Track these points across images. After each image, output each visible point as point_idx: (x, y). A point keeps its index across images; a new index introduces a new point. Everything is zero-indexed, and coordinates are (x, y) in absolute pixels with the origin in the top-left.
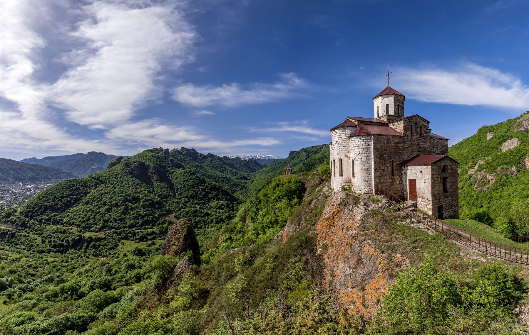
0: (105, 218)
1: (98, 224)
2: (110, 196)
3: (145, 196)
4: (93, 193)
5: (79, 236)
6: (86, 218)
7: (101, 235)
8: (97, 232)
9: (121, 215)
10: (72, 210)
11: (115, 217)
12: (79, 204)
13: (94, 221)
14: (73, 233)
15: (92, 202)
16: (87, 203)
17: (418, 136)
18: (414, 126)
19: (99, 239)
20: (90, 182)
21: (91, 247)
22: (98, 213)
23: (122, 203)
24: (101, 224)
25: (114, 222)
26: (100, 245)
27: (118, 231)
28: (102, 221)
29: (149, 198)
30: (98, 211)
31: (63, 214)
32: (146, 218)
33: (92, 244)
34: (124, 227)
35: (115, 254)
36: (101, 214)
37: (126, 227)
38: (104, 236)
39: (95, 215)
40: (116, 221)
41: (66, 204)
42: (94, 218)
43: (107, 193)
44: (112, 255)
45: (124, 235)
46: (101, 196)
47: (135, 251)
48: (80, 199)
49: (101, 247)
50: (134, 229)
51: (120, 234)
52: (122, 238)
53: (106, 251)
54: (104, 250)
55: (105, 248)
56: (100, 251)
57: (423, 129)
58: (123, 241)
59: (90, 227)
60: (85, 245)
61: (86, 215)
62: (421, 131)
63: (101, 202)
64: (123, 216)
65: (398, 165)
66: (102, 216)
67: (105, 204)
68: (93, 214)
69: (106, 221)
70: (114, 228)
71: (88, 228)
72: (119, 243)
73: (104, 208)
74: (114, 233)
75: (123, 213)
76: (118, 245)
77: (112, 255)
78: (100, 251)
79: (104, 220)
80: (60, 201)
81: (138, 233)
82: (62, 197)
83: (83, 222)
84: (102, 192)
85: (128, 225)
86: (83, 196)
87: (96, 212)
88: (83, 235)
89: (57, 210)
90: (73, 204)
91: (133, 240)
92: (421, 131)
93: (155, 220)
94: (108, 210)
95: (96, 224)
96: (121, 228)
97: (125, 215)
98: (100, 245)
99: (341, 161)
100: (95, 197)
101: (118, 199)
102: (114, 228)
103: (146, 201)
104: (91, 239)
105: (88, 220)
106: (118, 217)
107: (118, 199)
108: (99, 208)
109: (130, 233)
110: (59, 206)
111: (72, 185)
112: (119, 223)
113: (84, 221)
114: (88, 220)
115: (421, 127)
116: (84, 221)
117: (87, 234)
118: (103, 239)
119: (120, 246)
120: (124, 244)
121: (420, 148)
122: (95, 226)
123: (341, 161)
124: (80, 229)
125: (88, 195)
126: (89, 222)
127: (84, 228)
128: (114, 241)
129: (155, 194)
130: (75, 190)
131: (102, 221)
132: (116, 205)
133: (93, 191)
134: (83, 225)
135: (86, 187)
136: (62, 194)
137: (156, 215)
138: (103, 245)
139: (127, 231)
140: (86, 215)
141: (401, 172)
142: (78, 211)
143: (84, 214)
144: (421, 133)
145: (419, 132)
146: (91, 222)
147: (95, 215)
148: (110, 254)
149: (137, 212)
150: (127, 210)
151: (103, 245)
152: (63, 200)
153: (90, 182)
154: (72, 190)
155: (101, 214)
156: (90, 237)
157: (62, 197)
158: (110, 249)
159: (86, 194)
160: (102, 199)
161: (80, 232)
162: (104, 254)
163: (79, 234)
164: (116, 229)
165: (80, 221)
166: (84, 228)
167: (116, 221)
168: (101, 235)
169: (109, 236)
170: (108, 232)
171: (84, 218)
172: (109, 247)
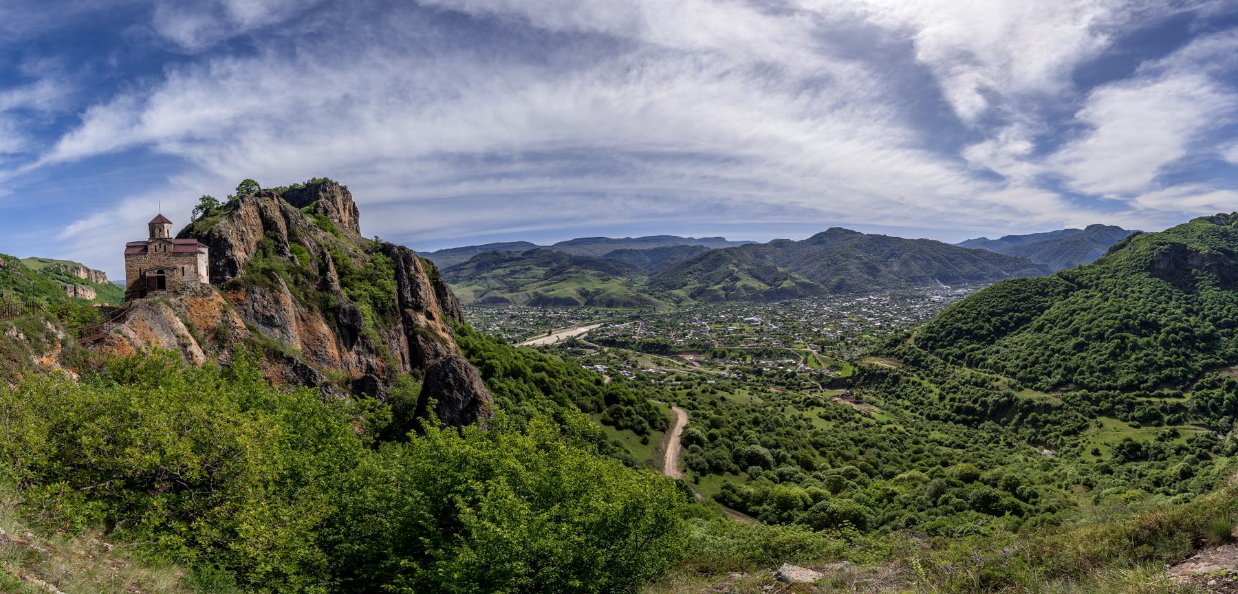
0: (1071, 364)
3: (1175, 319)
4: (1057, 308)
6: (1031, 359)
7: (1054, 399)
8: (1047, 392)
10: (1007, 340)
11: (1093, 364)
16: (1040, 329)
27: (1094, 395)
29: (1185, 325)
30: (1059, 346)
32: (1167, 372)
34: (1109, 388)
38: (1060, 402)
42: (1047, 361)
43: (1085, 310)
45: (1105, 405)
48: (1028, 320)
51: (1096, 402)
52: (1101, 413)
59: (1035, 380)
61: (1031, 354)
63: (1068, 329)
66: (1064, 359)
67: (1075, 332)
68: (1047, 353)
69: (1070, 371)
72: (1092, 423)
73: (1073, 341)
74: (1084, 398)
80: (989, 321)
82: (992, 314)
84: (1075, 306)
87: (1052, 350)
89: (980, 338)
90: (1013, 329)
91: (1125, 420)
93: (1190, 376)
94: (1080, 347)
95: (1049, 374)
96: (1102, 389)
97: (1116, 360)
103: (1175, 331)
105: (1033, 364)
108: (1063, 340)
112: (1098, 377)
113: (1025, 367)
114: (1033, 364)
116: (1025, 367)
120: (1101, 426)
122: (1045, 378)
125: (1046, 312)
128: (1080, 415)
129: (1205, 317)
130: (1019, 301)
131: (1061, 370)
133: (1057, 304)
134: (1021, 374)
135: (1044, 294)
137: (1197, 366)
140: (1031, 354)
142: (1018, 344)
143: (1027, 352)
146: (1038, 368)
149: (1147, 355)
152: (994, 319)
155: (1064, 353)
157: (992, 314)
159: (1042, 310)
160: (1071, 322)
164: (1090, 390)
167: (1092, 373)
168: (1054, 399)
169: (1071, 404)
170: (1072, 394)
171: (1025, 360)
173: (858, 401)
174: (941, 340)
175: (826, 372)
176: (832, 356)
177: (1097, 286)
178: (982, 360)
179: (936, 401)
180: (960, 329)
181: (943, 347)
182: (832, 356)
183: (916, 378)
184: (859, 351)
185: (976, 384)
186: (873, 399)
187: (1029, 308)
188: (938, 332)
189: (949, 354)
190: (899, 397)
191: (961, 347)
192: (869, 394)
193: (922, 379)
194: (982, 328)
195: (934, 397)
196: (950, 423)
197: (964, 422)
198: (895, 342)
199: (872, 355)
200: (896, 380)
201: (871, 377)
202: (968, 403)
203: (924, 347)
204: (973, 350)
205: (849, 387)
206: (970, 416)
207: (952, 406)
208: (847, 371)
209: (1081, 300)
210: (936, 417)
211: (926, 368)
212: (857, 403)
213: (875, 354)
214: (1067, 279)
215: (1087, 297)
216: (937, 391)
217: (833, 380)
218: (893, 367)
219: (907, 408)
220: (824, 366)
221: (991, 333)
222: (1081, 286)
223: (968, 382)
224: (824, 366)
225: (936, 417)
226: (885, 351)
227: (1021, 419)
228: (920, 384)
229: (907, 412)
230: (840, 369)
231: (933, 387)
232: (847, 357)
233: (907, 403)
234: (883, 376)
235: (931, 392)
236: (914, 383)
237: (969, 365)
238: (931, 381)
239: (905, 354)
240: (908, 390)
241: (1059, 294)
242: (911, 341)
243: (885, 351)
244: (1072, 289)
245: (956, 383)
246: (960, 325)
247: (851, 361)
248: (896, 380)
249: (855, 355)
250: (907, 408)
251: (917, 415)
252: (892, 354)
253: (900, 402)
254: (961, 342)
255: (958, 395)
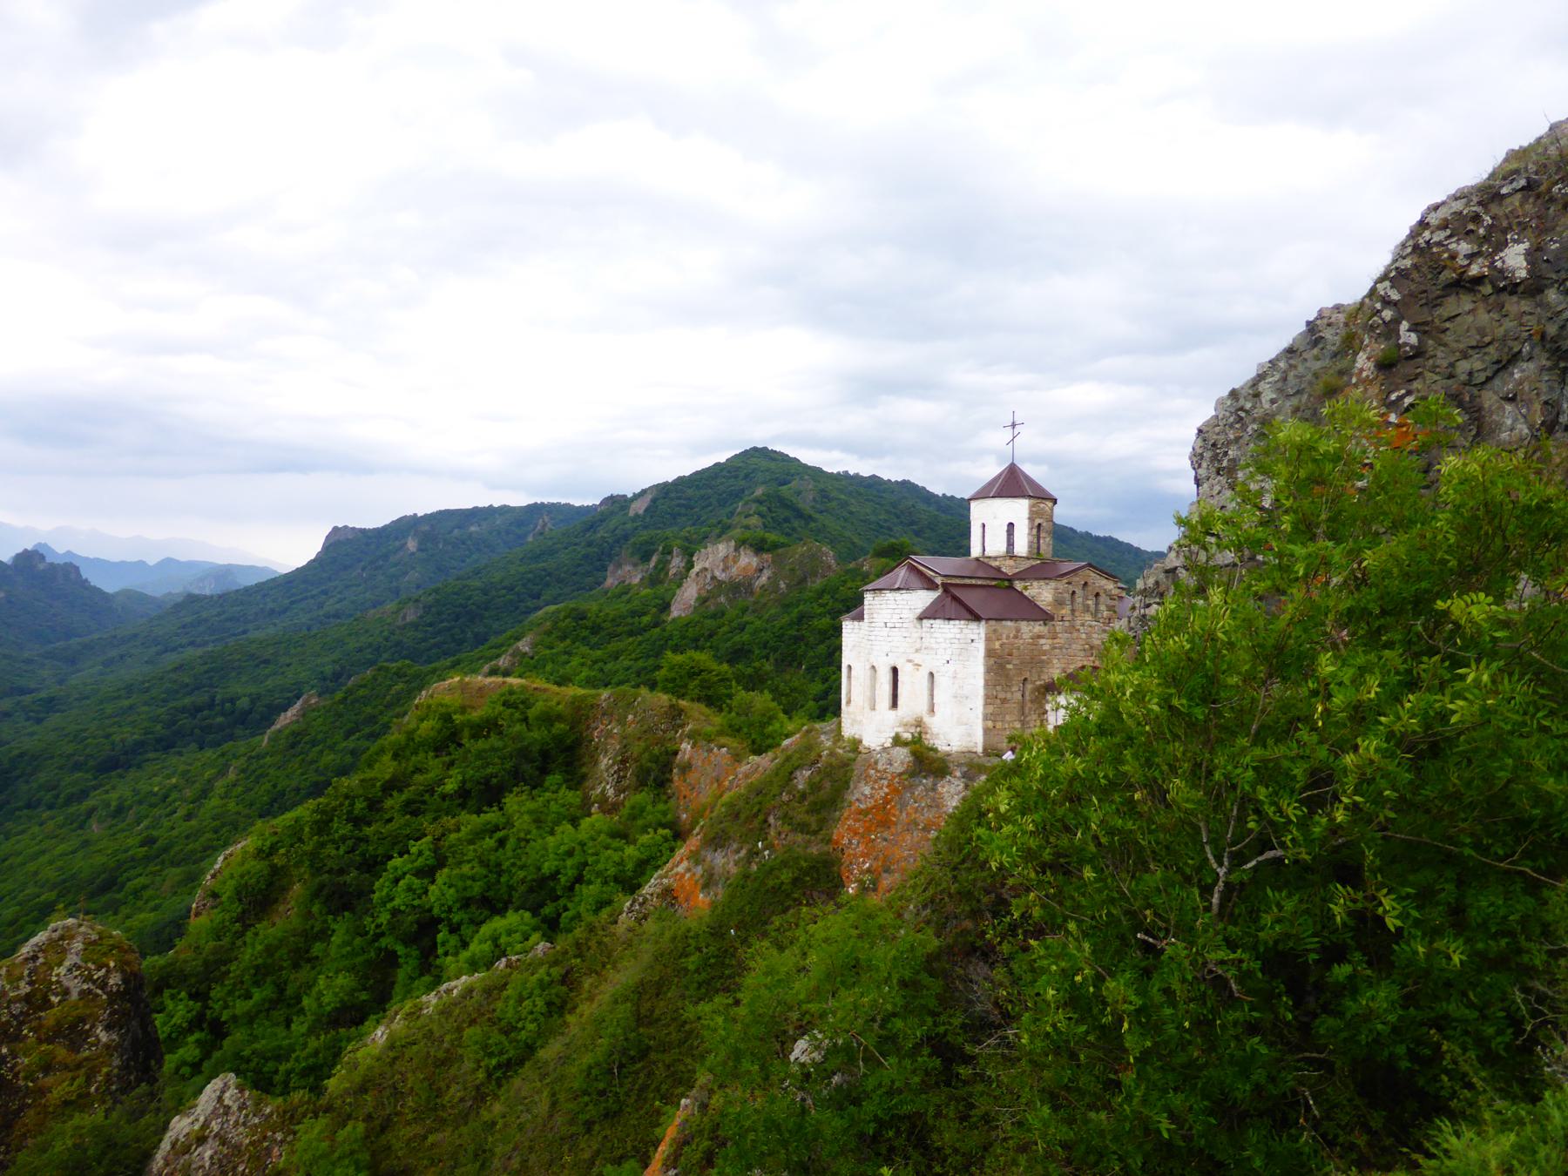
17: (1088, 617)
18: (1079, 592)
57: (1103, 598)
62: (1097, 604)
65: (1038, 689)
92: (1097, 604)
99: (895, 671)
115: (1097, 595)
121: (1092, 648)
123: (895, 671)
141: (1042, 706)
144: (1097, 610)
145: (1092, 608)
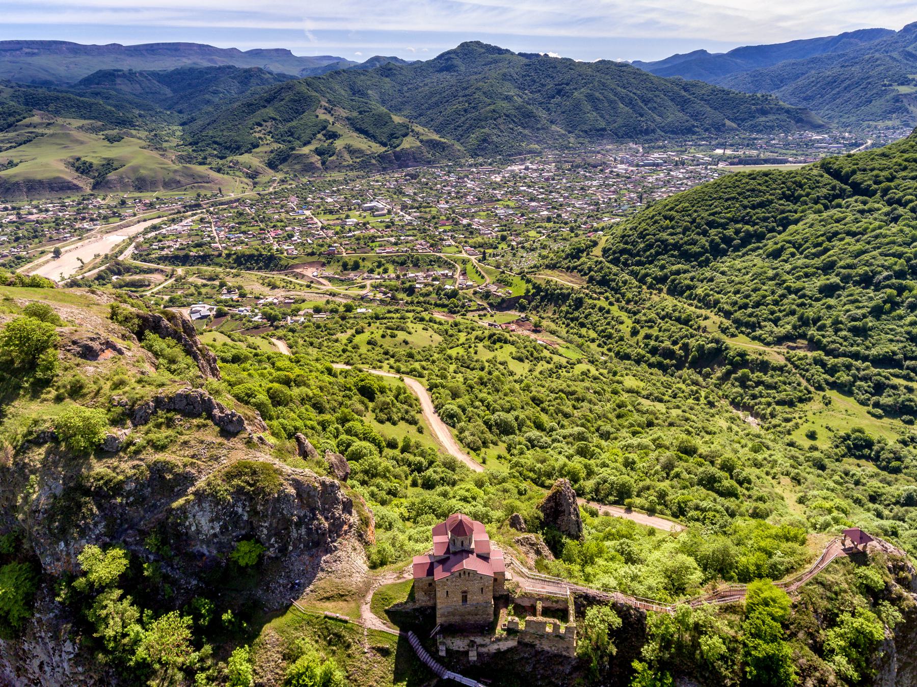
0: (810, 313)
1: (781, 323)
2: (858, 246)
4: (808, 224)
5: (717, 341)
6: (755, 297)
7: (775, 356)
8: (768, 344)
9: (864, 316)
10: (725, 263)
11: (843, 318)
12: (754, 250)
13: (772, 313)
14: (704, 331)
15: (793, 255)
16: (776, 254)
19: (764, 366)
20: (816, 185)
21: (736, 379)
22: (796, 291)
23: (887, 278)
24: (789, 327)
25: (830, 331)
26: (759, 383)
27: (831, 361)
28: (793, 319)
30: (799, 284)
31: (700, 271)
33: (740, 373)
34: (856, 356)
35: (787, 420)
36: (804, 296)
37: (865, 359)
38: (782, 361)
39: (783, 296)
40: (837, 331)
41: (718, 245)
42: (776, 303)
43: (853, 234)
44: (775, 421)
45: (844, 377)
46: (829, 239)
47: (848, 437)
48: (760, 237)
49: (761, 388)
50: (885, 372)
51: (832, 371)
52: (833, 386)
53: (769, 404)
54: (763, 400)
55: (769, 395)
56: (754, 397)
58: (833, 394)
59: (753, 326)
60: (724, 369)
61: (755, 290)
63: (817, 262)
64: (870, 322)
66: (802, 305)
67: (828, 268)
68: (780, 292)
69: (805, 322)
70: (823, 348)
71: (750, 327)
72: (818, 396)
73: (821, 281)
74: (818, 362)
75: (877, 312)
76: (810, 399)
77: (775, 421)
78: (754, 397)
79: (801, 318)
80: (705, 233)
81: (894, 387)
82: (711, 224)
83: (740, 308)
84: (838, 227)
85: (874, 352)
86: (772, 230)
87: (788, 289)
88: (729, 342)
89: (687, 256)
90: (737, 249)
94: (829, 291)
95: (776, 322)
96: (844, 355)
98: (759, 383)
100: (806, 240)
101: (881, 260)
102: (823, 348)
104: (742, 360)
105: (757, 305)
106: (854, 319)
107: (881, 260)
108: (807, 275)
109: (865, 379)
110: (696, 249)
111: (753, 190)
112: (845, 338)
113: (745, 306)
114: (757, 305)
116: (745, 306)
117: (740, 343)
118: (774, 369)
119: (816, 405)
122: (769, 326)
124: (727, 323)
125: (792, 228)
126: (757, 311)
127: (738, 323)
128: (804, 383)
130: (754, 207)
131: (793, 319)
132: (866, 281)
133: (811, 217)
134: (738, 315)
135: (795, 199)
136: (713, 214)
138: (769, 387)
139: (858, 369)
140: (755, 290)
142: (742, 269)
143: (752, 285)
146: (763, 311)
147: (783, 296)
148: (773, 416)
150: (895, 305)
151: (769, 387)
152: (713, 232)
153: (816, 185)
154: (745, 207)
155: (804, 296)
156: (742, 355)
157: (711, 224)
158: (781, 403)
159: (785, 223)
160: (826, 250)
161: (724, 331)
162: (759, 408)
163: (718, 335)
164: (829, 353)
165: (735, 303)
166: (738, 323)
167: (837, 331)
168: (775, 356)
169: (797, 367)
170: (801, 353)
171: (747, 297)
172: (783, 396)
173: (537, 329)
174: (638, 254)
175: (493, 288)
176: (498, 267)
177: (885, 191)
178: (689, 288)
179: (627, 335)
180: (664, 242)
181: (639, 263)
182: (498, 267)
183: (602, 303)
184: (532, 259)
185: (678, 320)
186: (553, 326)
187: (765, 219)
188: (634, 243)
189: (647, 275)
190: (582, 325)
191: (663, 267)
192: (548, 318)
193: (611, 304)
194: (694, 243)
195: (626, 328)
196: (644, 365)
197: (660, 366)
198: (576, 253)
199: (548, 267)
200: (579, 303)
201: (549, 297)
202: (667, 344)
203: (615, 262)
204: (678, 273)
205: (523, 309)
206: (667, 360)
207: (647, 345)
208: (519, 289)
209: (850, 217)
210: (627, 357)
211: (616, 290)
212: (536, 331)
213: (552, 267)
214: (836, 174)
215: (862, 212)
216: (629, 322)
217: (503, 300)
218: (576, 287)
219: (593, 341)
220: (489, 279)
221: (706, 251)
222: (858, 190)
223: (669, 316)
224: (489, 279)
225: (627, 357)
226: (565, 263)
227: (725, 377)
228: (608, 312)
229: (593, 346)
230: (509, 284)
231: (624, 316)
232: (516, 270)
233: (593, 334)
234: (565, 297)
235: (622, 323)
236: (601, 309)
237: (671, 292)
238: (621, 308)
239: (590, 269)
240: (594, 318)
241: (816, 202)
242: (597, 251)
243: (565, 263)
244: (842, 195)
245: (653, 316)
246: (664, 235)
247: (522, 275)
248: (579, 303)
249: (525, 266)
250: (593, 341)
251: (605, 350)
252: (575, 268)
253: (583, 331)
254: (663, 260)
255: (654, 332)
